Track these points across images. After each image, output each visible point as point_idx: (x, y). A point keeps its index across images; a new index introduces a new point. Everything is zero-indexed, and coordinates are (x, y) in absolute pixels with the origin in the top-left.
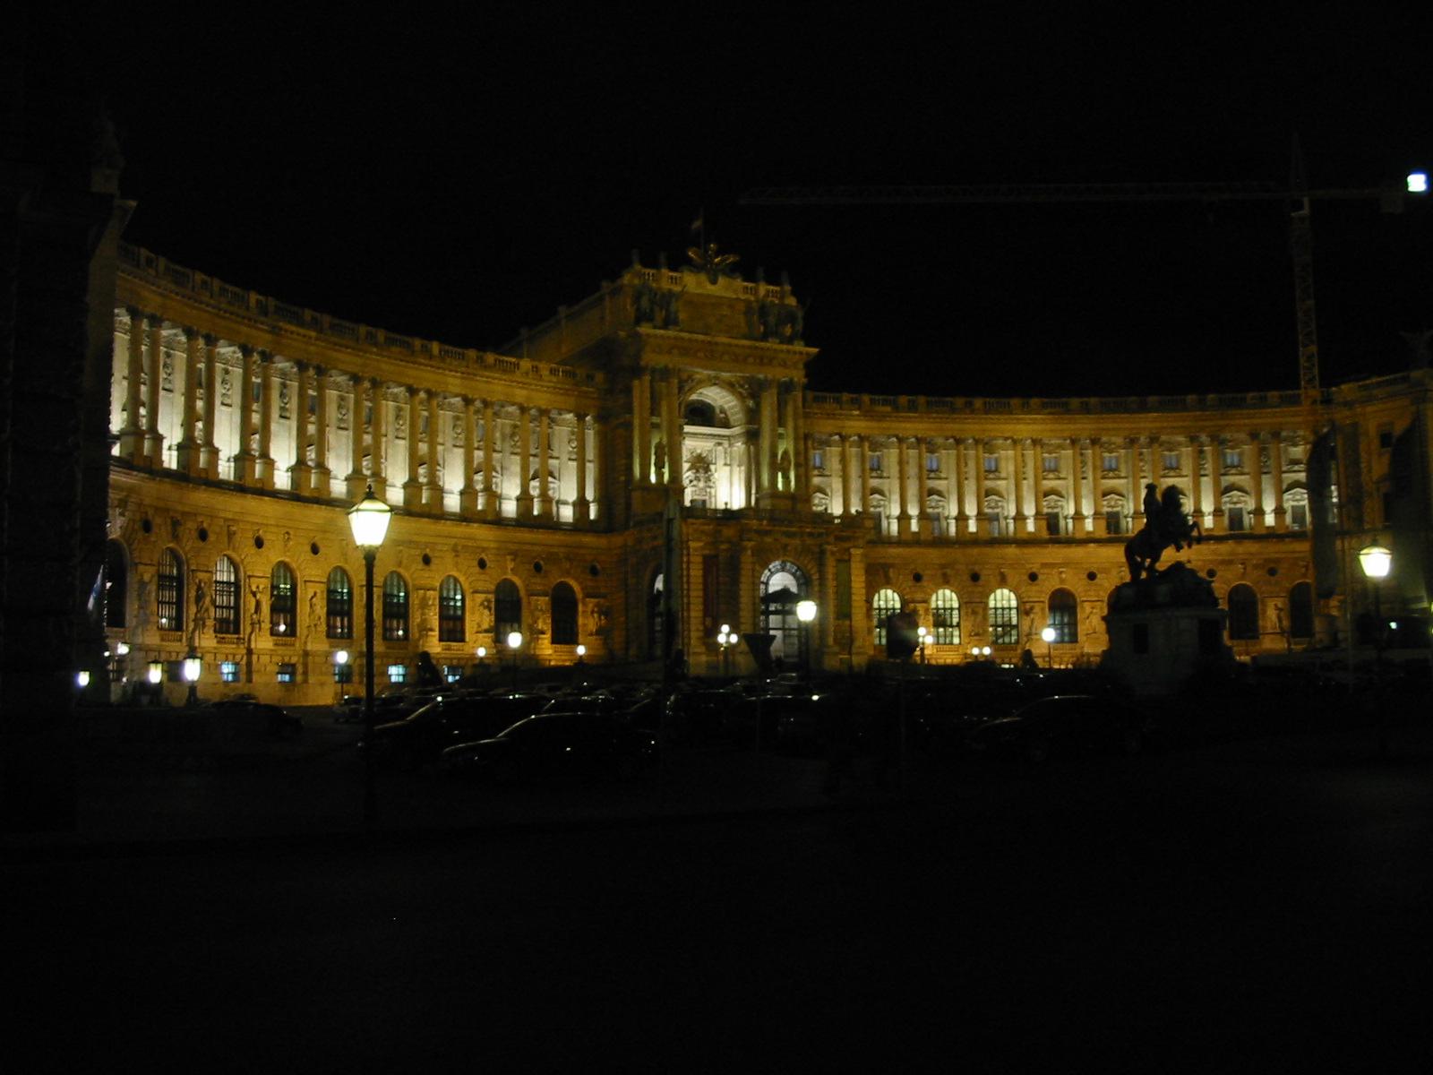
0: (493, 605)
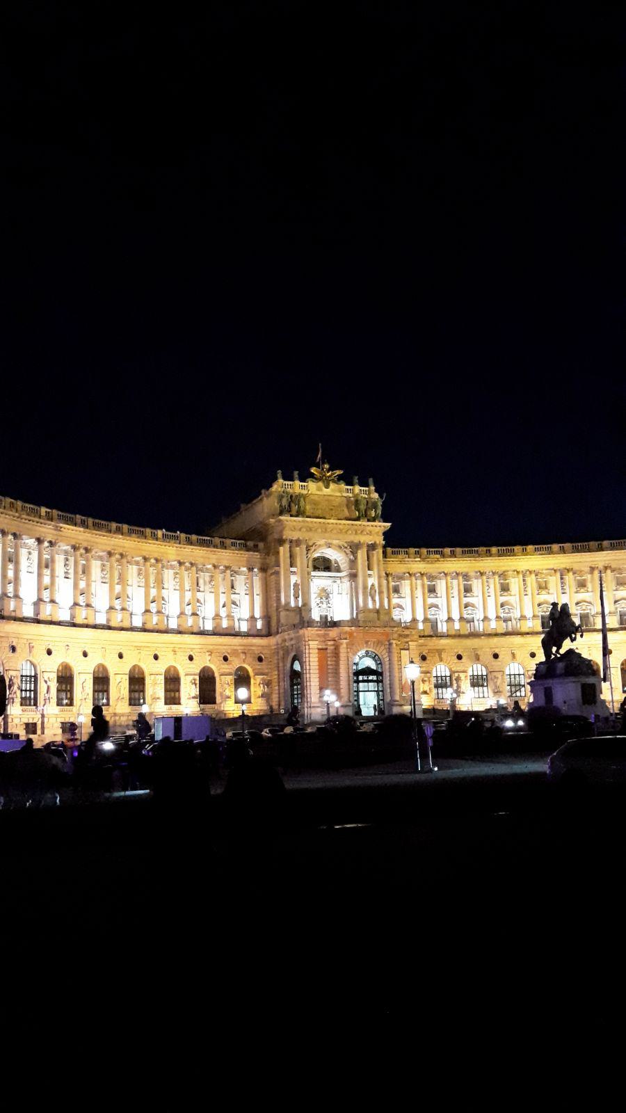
0: (198, 682)
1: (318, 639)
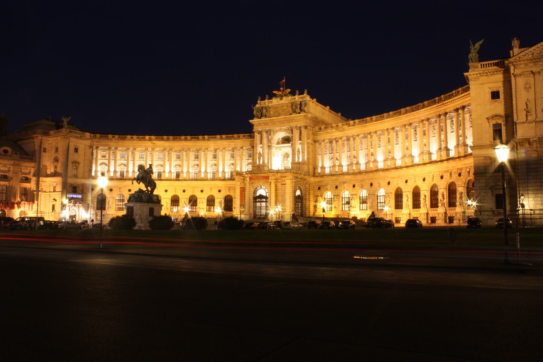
0: (223, 202)
1: (241, 181)
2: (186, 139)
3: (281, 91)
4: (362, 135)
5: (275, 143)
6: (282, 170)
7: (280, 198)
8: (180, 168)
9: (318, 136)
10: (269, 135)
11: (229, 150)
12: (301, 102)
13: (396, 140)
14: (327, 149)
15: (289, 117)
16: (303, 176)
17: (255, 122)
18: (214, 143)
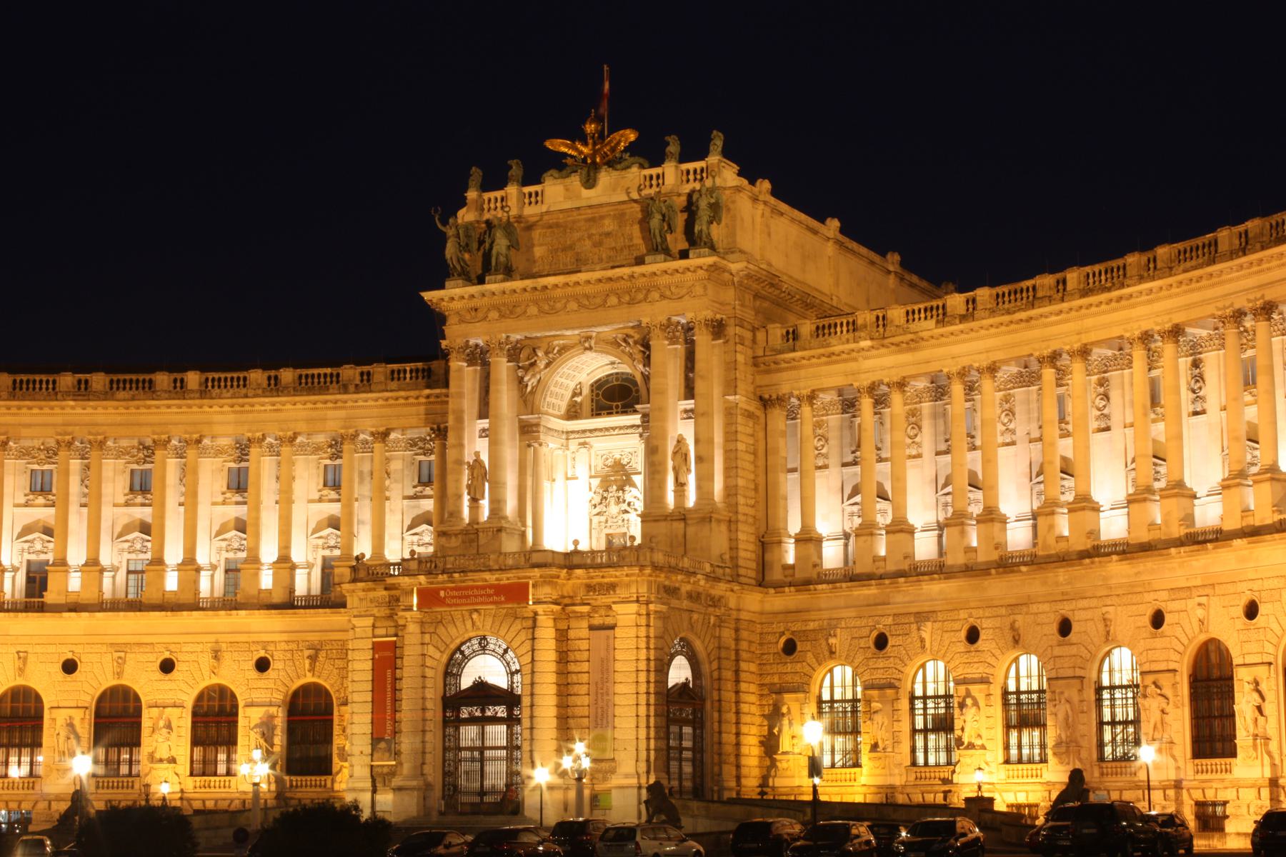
1: (375, 611)
2: (82, 392)
3: (590, 141)
4: (1014, 369)
5: (556, 412)
6: (593, 552)
7: (582, 701)
8: (51, 546)
9: (785, 375)
10: (526, 369)
11: (317, 449)
12: (690, 196)
13: (1194, 391)
14: (827, 440)
15: (632, 276)
16: (702, 583)
17: (452, 299)
18: (237, 408)
